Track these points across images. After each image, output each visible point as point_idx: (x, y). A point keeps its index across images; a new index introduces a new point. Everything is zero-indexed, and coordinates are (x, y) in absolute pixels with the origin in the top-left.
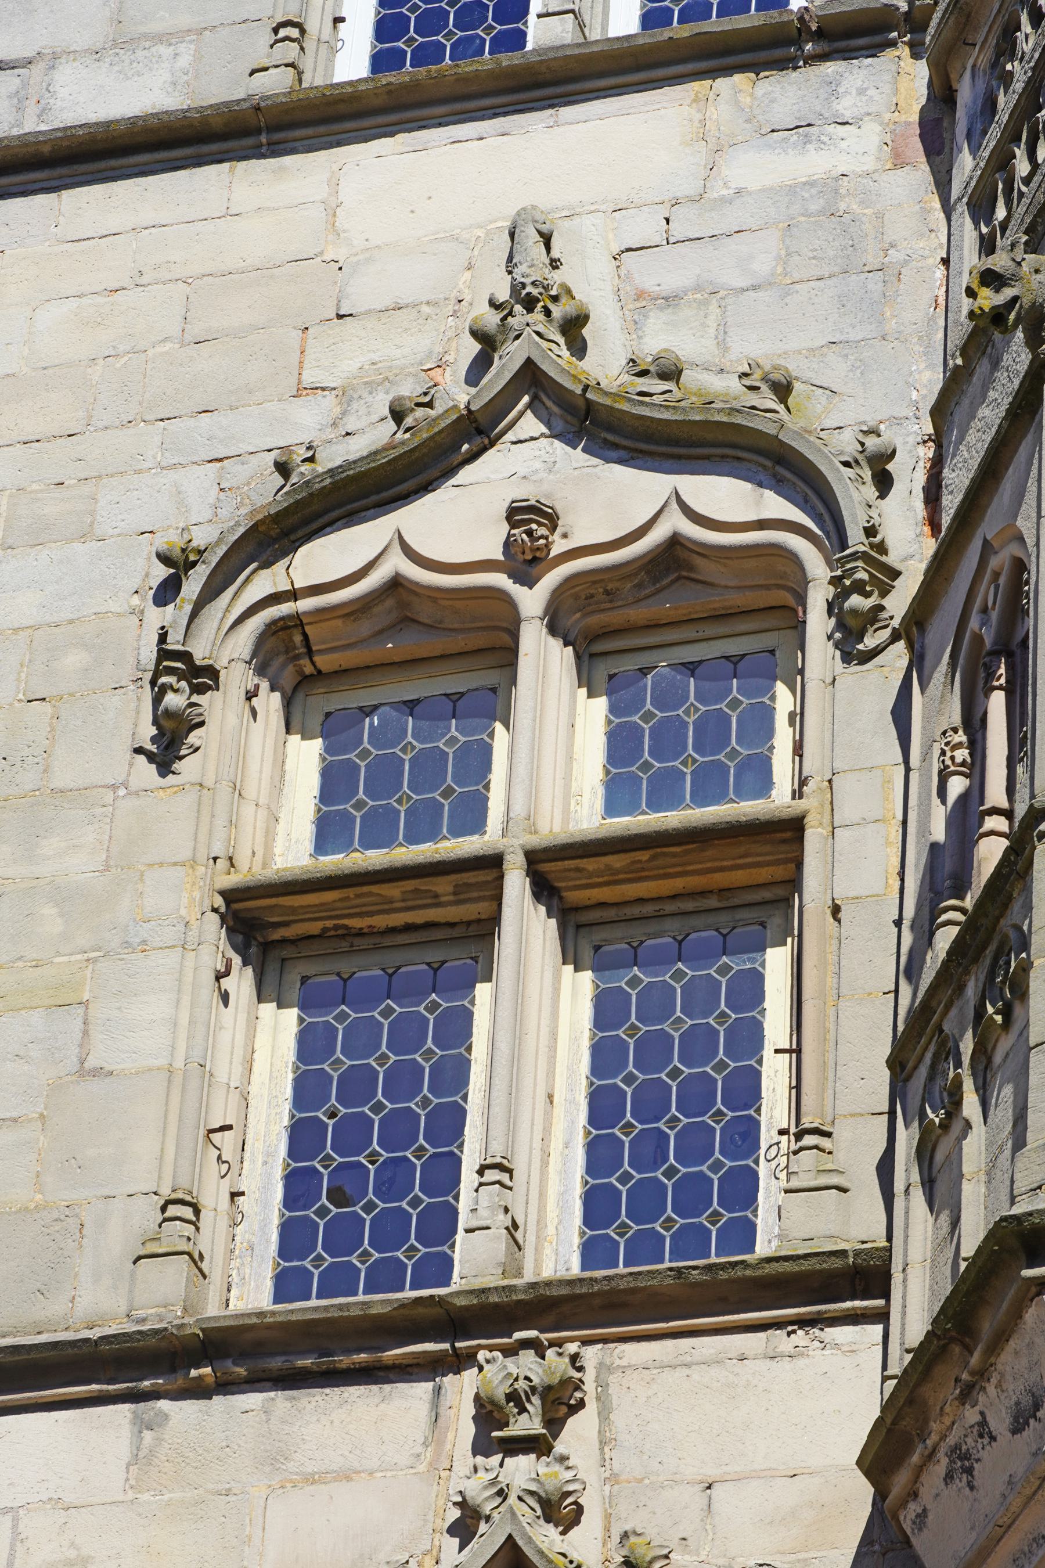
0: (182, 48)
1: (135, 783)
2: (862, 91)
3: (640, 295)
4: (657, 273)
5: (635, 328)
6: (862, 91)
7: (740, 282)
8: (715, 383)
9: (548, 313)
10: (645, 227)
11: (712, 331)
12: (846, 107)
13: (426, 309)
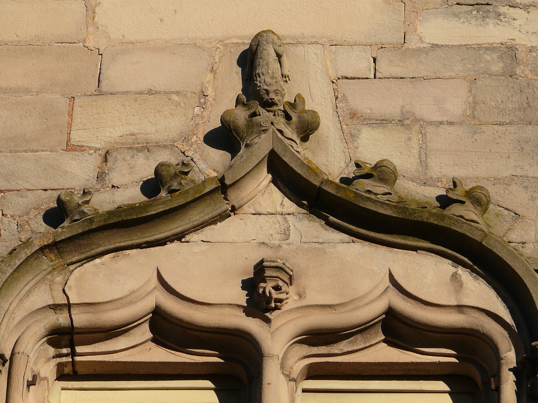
3: (353, 115)
4: (368, 100)
5: (349, 138)
7: (437, 118)
8: (418, 190)
10: (358, 63)
11: (415, 151)
13: (175, 97)
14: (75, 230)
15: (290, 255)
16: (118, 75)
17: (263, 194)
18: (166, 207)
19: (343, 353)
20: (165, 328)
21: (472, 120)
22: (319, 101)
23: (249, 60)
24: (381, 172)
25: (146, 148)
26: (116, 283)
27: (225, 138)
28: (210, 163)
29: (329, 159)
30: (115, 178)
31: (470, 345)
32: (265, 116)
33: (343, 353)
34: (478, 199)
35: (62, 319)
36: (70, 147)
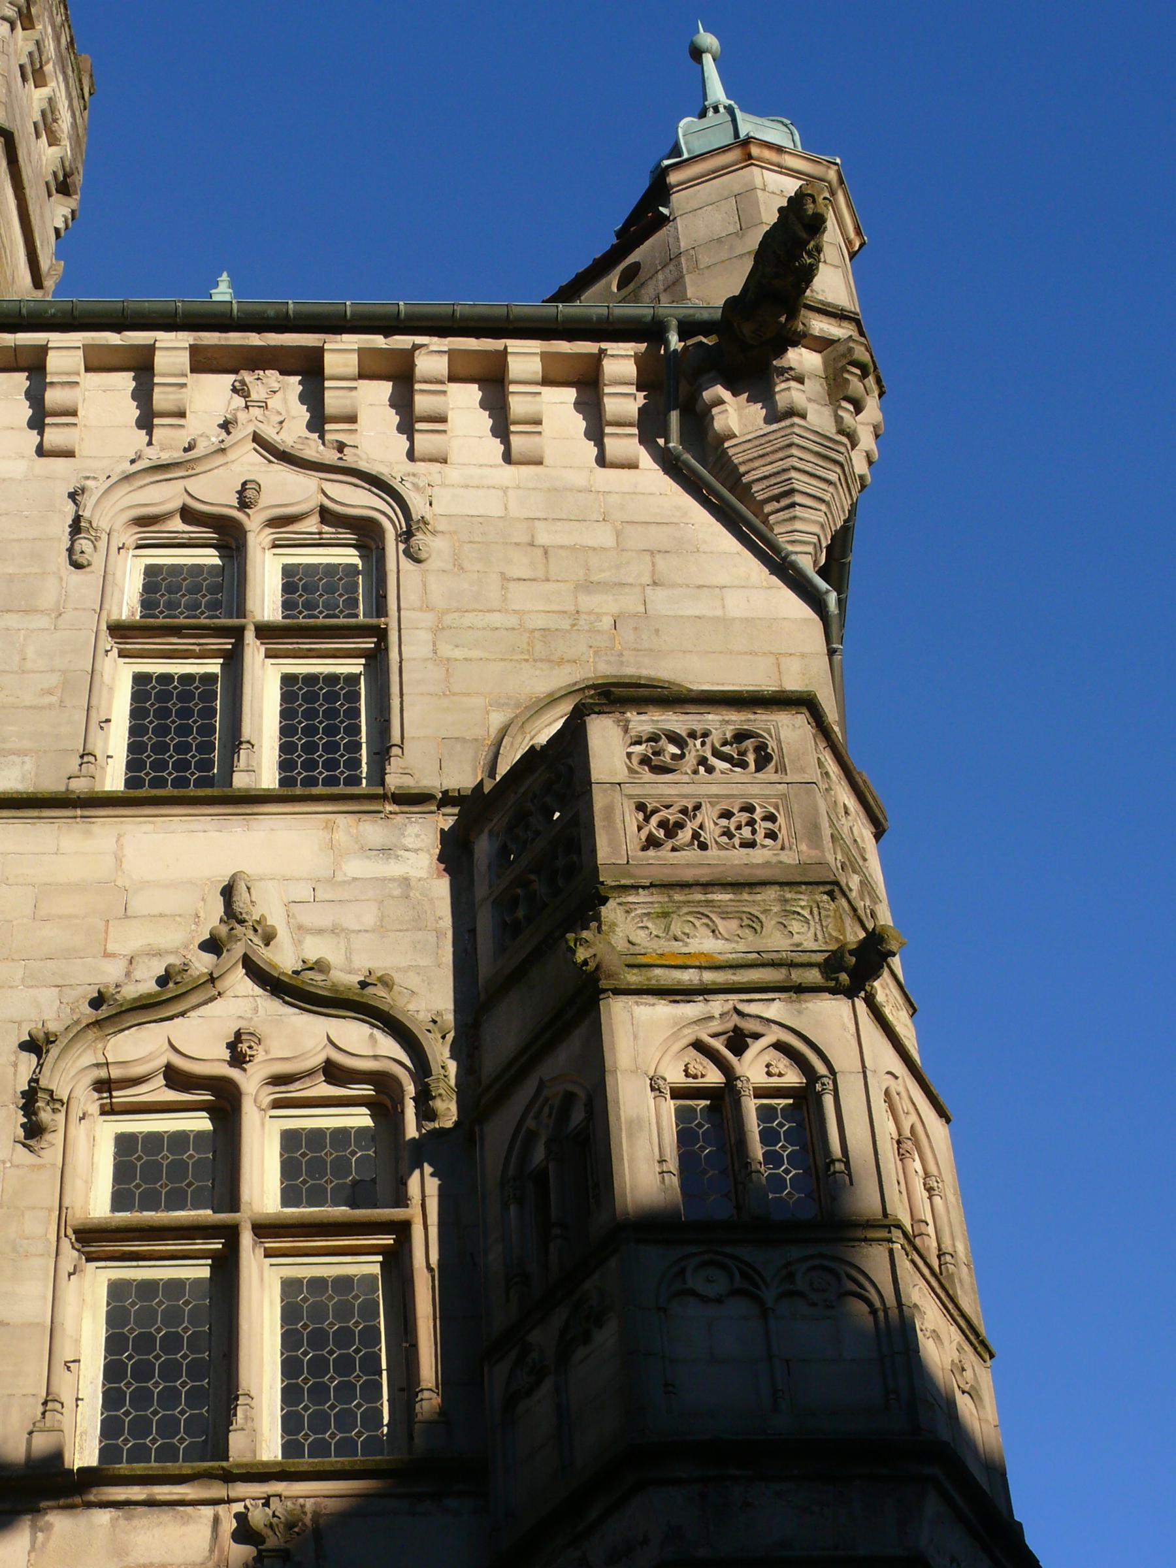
0: (27, 759)
1: (16, 1161)
2: (417, 836)
3: (300, 927)
5: (297, 943)
6: (417, 836)
7: (358, 928)
8: (345, 977)
9: (255, 930)
10: (303, 892)
12: (409, 842)
13: (178, 918)
14: (110, 1012)
15: (258, 1024)
16: (139, 904)
17: (239, 983)
18: (172, 994)
19: (296, 1091)
20: (174, 1077)
21: (381, 929)
22: (276, 919)
23: (228, 892)
24: (320, 966)
25: (159, 954)
26: (140, 1047)
27: (213, 945)
28: (203, 963)
29: (284, 958)
30: (137, 975)
31: (383, 1082)
32: (239, 929)
33: (296, 1091)
34: (386, 982)
35: (102, 1073)
36: (107, 955)
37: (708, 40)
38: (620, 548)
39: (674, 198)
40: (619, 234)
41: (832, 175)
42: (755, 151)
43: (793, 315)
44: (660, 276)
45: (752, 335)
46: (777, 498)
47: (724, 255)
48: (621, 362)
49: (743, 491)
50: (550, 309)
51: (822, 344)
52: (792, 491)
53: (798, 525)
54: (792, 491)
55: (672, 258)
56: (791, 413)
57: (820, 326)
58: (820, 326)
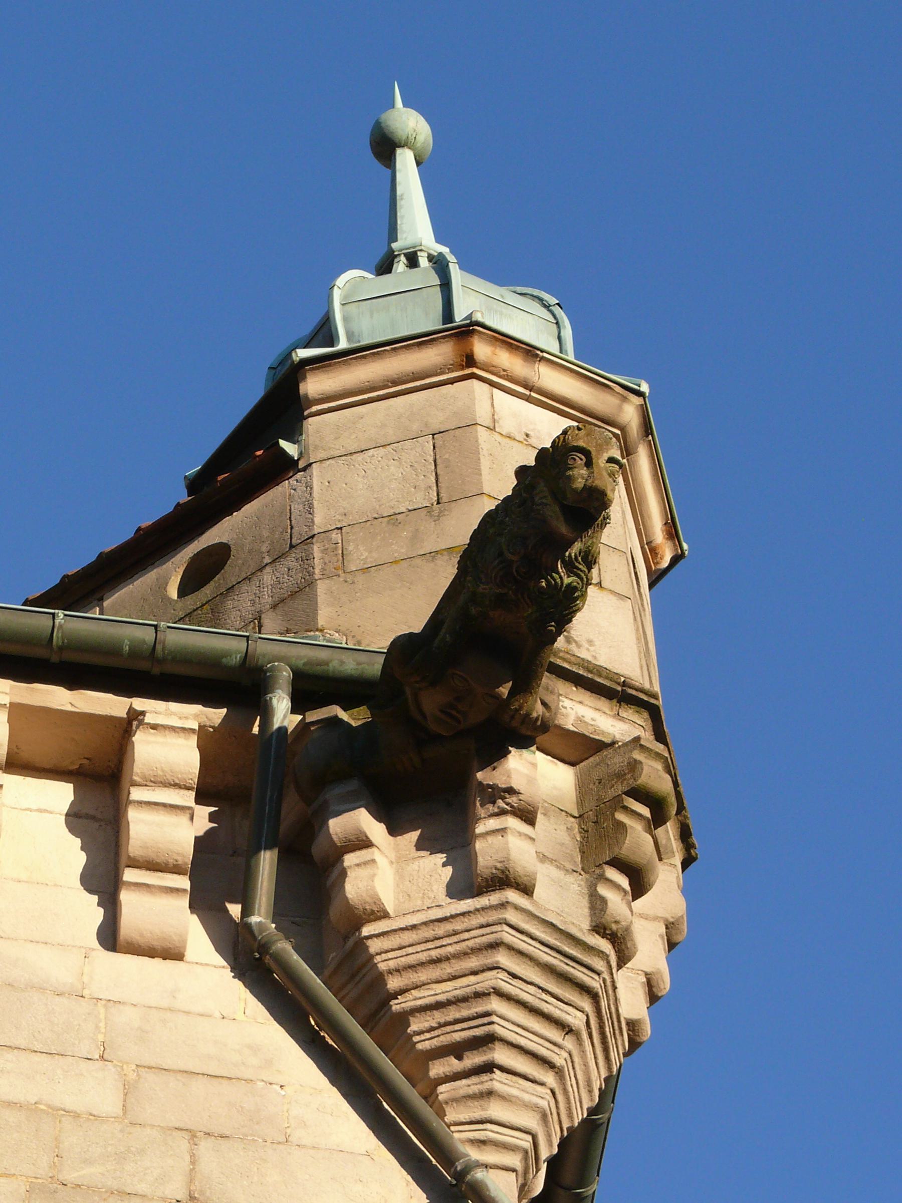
37: (409, 123)
38: (128, 1117)
39: (312, 425)
40: (194, 485)
41: (630, 414)
42: (482, 350)
43: (525, 684)
44: (267, 577)
45: (437, 718)
46: (457, 1050)
47: (399, 549)
48: (170, 740)
49: (390, 1027)
50: (39, 621)
51: (579, 748)
52: (490, 1039)
53: (496, 1110)
54: (490, 1039)
55: (296, 544)
56: (503, 879)
57: (577, 711)
58: (577, 711)
